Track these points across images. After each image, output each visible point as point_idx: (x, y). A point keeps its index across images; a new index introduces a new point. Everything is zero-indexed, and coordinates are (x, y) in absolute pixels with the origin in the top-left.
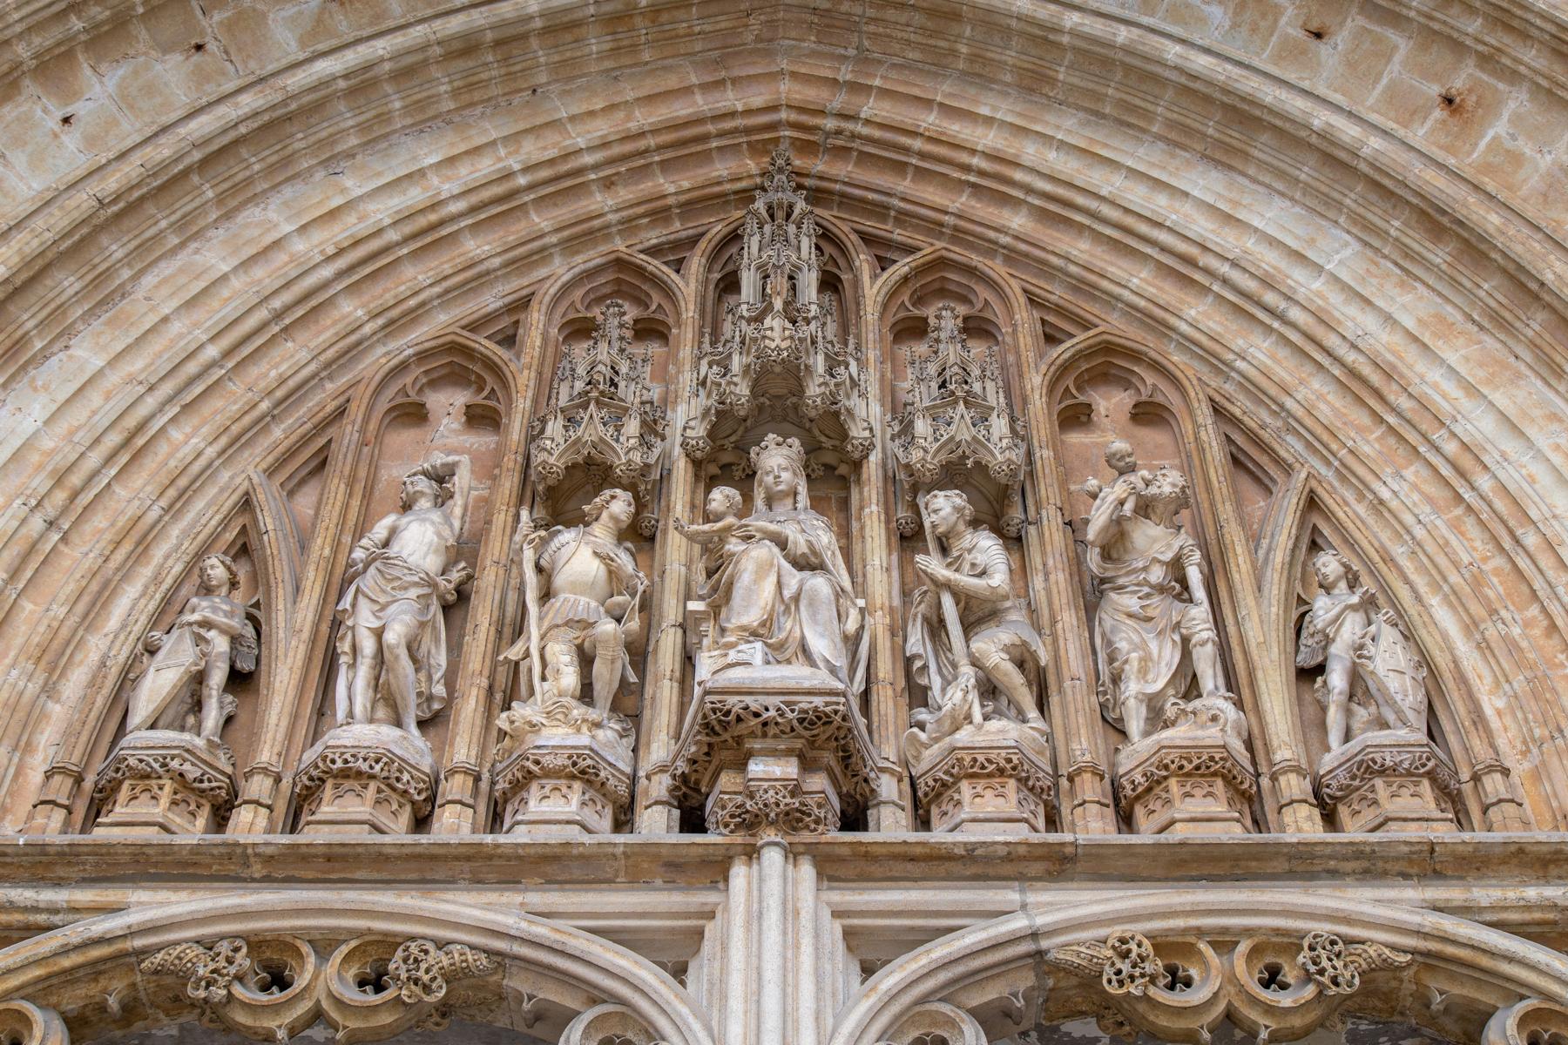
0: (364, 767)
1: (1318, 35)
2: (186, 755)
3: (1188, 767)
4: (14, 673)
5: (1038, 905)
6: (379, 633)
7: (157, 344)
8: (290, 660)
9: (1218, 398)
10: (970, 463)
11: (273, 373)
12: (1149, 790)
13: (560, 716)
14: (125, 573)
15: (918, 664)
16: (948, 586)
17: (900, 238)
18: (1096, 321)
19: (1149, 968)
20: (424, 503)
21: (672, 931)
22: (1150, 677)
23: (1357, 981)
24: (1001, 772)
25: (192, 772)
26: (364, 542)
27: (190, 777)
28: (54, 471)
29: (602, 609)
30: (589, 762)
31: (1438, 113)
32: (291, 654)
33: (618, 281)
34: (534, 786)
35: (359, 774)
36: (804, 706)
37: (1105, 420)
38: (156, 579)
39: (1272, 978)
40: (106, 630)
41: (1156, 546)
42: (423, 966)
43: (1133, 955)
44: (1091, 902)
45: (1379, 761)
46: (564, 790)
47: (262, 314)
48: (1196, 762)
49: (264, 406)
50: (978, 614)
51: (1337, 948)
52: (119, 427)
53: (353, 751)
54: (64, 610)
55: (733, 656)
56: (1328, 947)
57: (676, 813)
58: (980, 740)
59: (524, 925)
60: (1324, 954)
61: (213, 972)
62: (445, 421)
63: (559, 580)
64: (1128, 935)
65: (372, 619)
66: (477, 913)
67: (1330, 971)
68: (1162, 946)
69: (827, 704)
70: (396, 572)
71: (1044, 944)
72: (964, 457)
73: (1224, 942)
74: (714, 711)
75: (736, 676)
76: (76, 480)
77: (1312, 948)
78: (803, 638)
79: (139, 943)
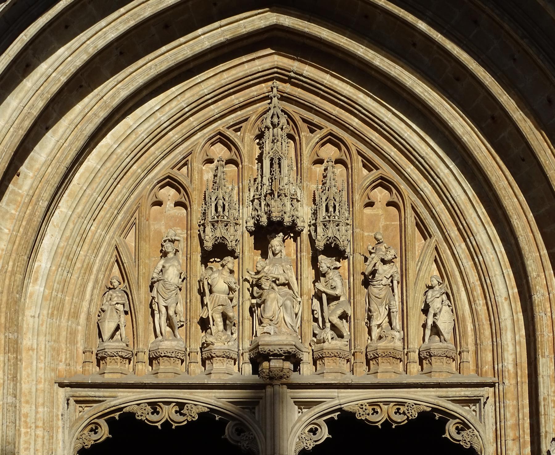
0: (169, 355)
1: (458, 79)
2: (123, 350)
3: (384, 355)
4: (70, 322)
5: (342, 396)
6: (166, 307)
7: (84, 200)
8: (141, 313)
9: (413, 205)
10: (333, 245)
11: (117, 200)
12: (374, 358)
13: (219, 340)
14: (88, 280)
15: (315, 312)
16: (324, 292)
17: (316, 123)
18: (379, 167)
19: (367, 412)
20: (171, 255)
21: (251, 401)
22: (379, 319)
23: (416, 416)
24: (335, 356)
25: (124, 354)
26: (156, 270)
27: (124, 356)
28: (66, 256)
29: (227, 298)
30: (228, 353)
31: (489, 121)
32: (141, 311)
33: (219, 138)
34: (214, 359)
35: (168, 357)
36: (284, 350)
37: (379, 203)
38: (96, 281)
39: (398, 412)
40: (86, 300)
41: (386, 273)
42: (192, 412)
43: (364, 409)
44: (355, 396)
45: (433, 353)
46: (222, 361)
47: (112, 180)
48: (386, 354)
49: (116, 212)
50: (332, 299)
51: (413, 407)
52: (79, 234)
53: (167, 350)
54: (77, 299)
55: (265, 330)
56: (411, 406)
57: (251, 365)
58: (330, 346)
59: (216, 402)
60: (410, 408)
61: (142, 413)
62: (168, 203)
63: (214, 289)
64: (363, 404)
65: (163, 302)
66: (204, 399)
67: (411, 413)
68: (371, 404)
69: (290, 348)
70: (167, 286)
71: (342, 406)
72: (331, 243)
73: (387, 403)
74: (262, 351)
75: (267, 339)
76: (71, 256)
77: (408, 406)
78: (284, 317)
79: (122, 406)
